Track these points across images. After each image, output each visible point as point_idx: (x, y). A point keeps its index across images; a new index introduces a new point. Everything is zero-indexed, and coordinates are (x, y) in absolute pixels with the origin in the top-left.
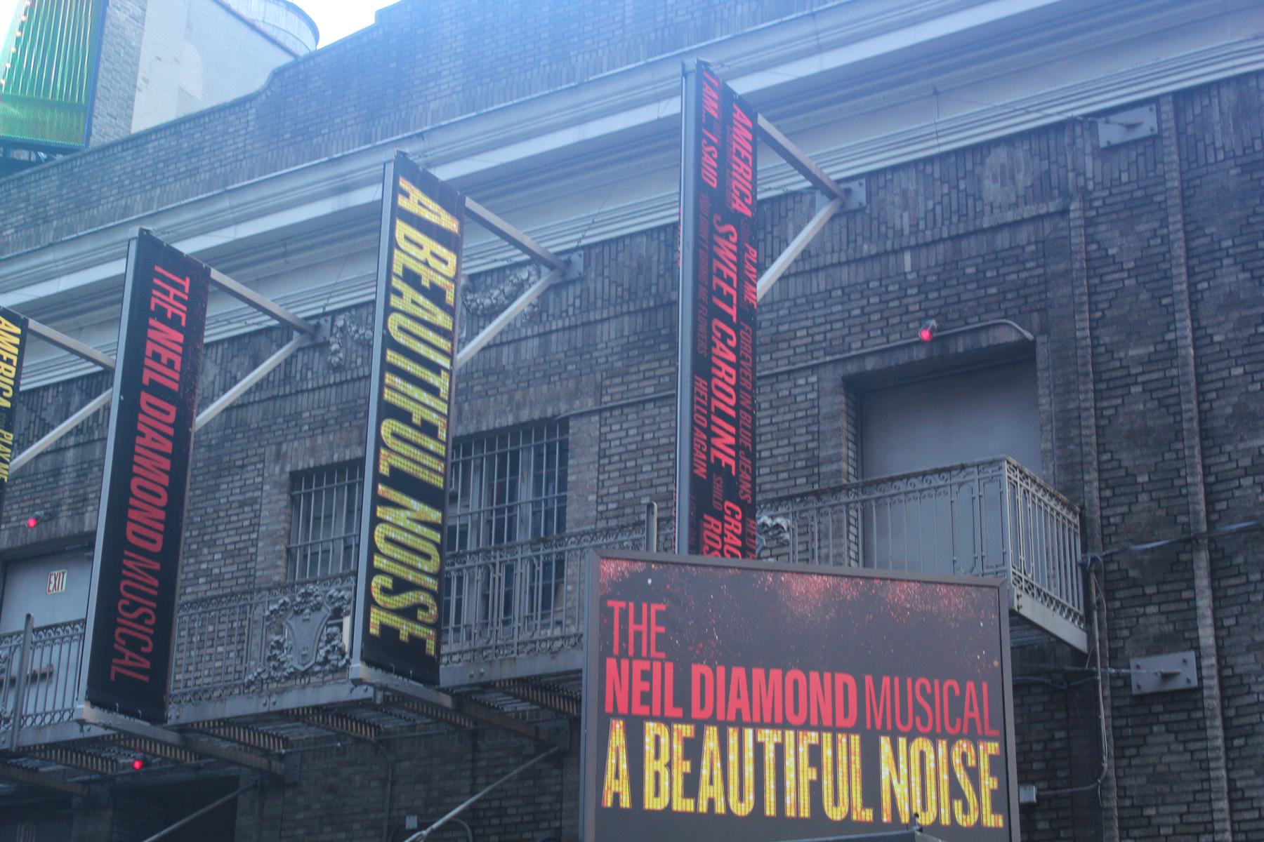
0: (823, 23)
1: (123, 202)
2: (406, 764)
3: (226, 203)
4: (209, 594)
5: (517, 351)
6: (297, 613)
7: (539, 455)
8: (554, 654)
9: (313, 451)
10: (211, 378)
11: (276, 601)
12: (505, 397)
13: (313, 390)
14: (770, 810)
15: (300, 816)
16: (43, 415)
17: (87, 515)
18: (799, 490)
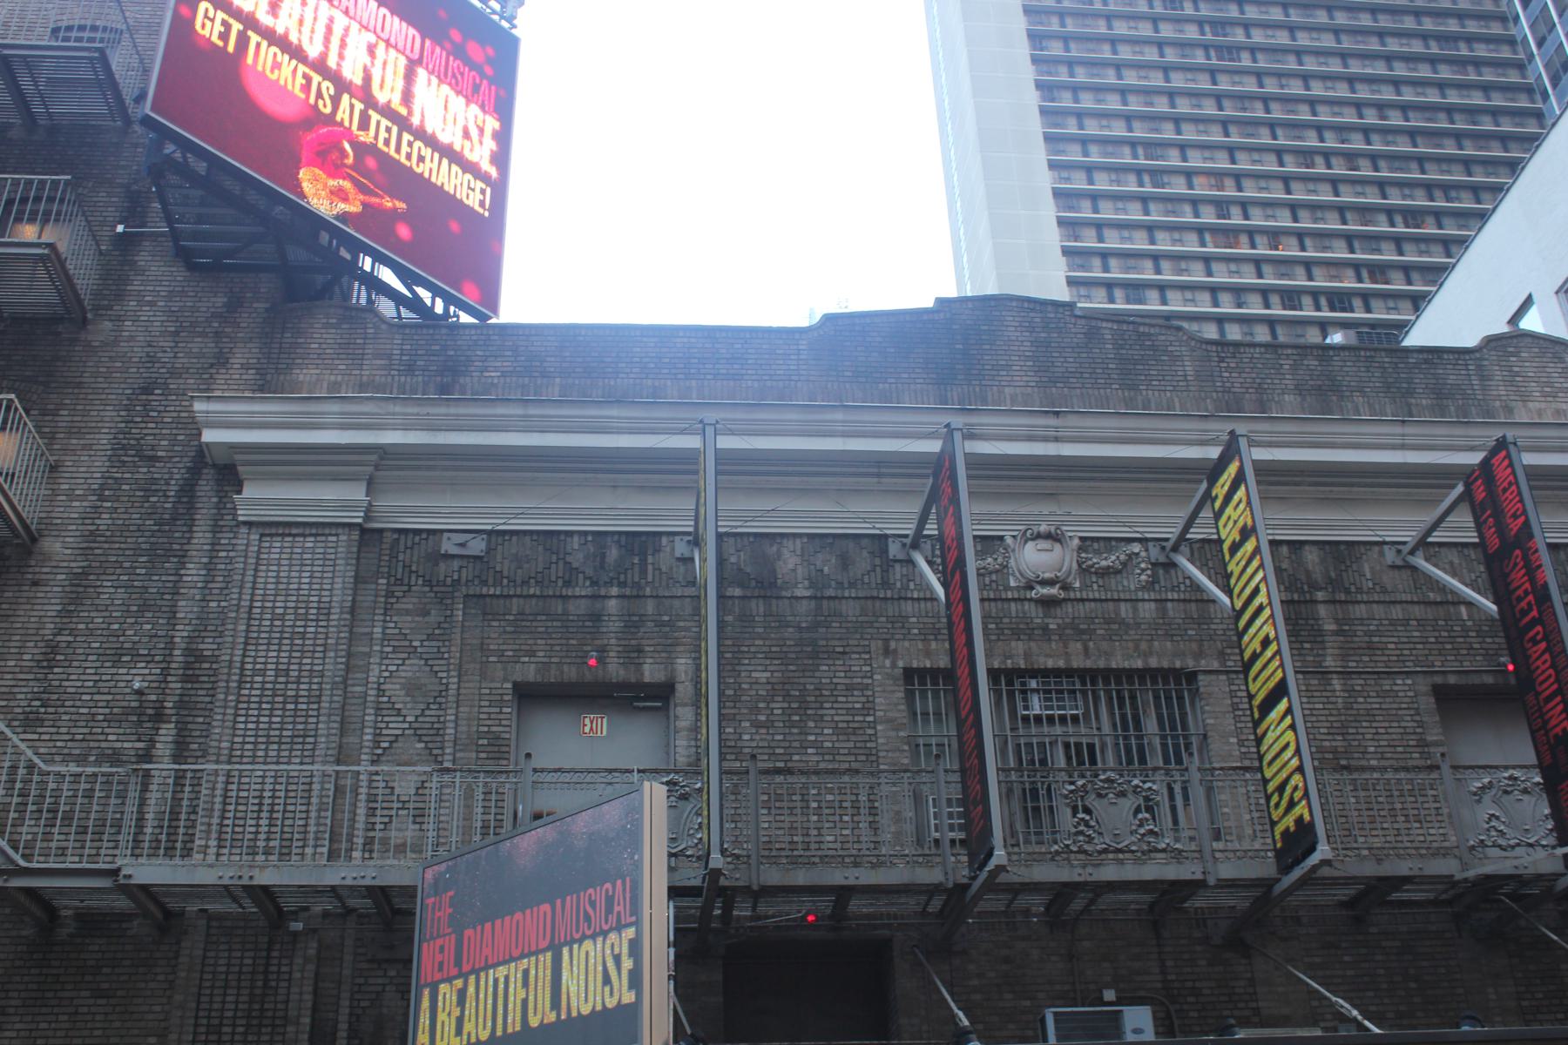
0: (1409, 430)
1: (650, 382)
2: (1086, 944)
3: (839, 416)
4: (822, 765)
5: (1135, 610)
6: (1100, 796)
7: (1157, 698)
8: (1379, 861)
9: (928, 653)
10: (791, 566)
11: (1072, 783)
12: (1131, 645)
13: (918, 599)
14: (499, 1033)
15: (975, 982)
16: (569, 559)
17: (646, 667)
18: (1410, 763)
